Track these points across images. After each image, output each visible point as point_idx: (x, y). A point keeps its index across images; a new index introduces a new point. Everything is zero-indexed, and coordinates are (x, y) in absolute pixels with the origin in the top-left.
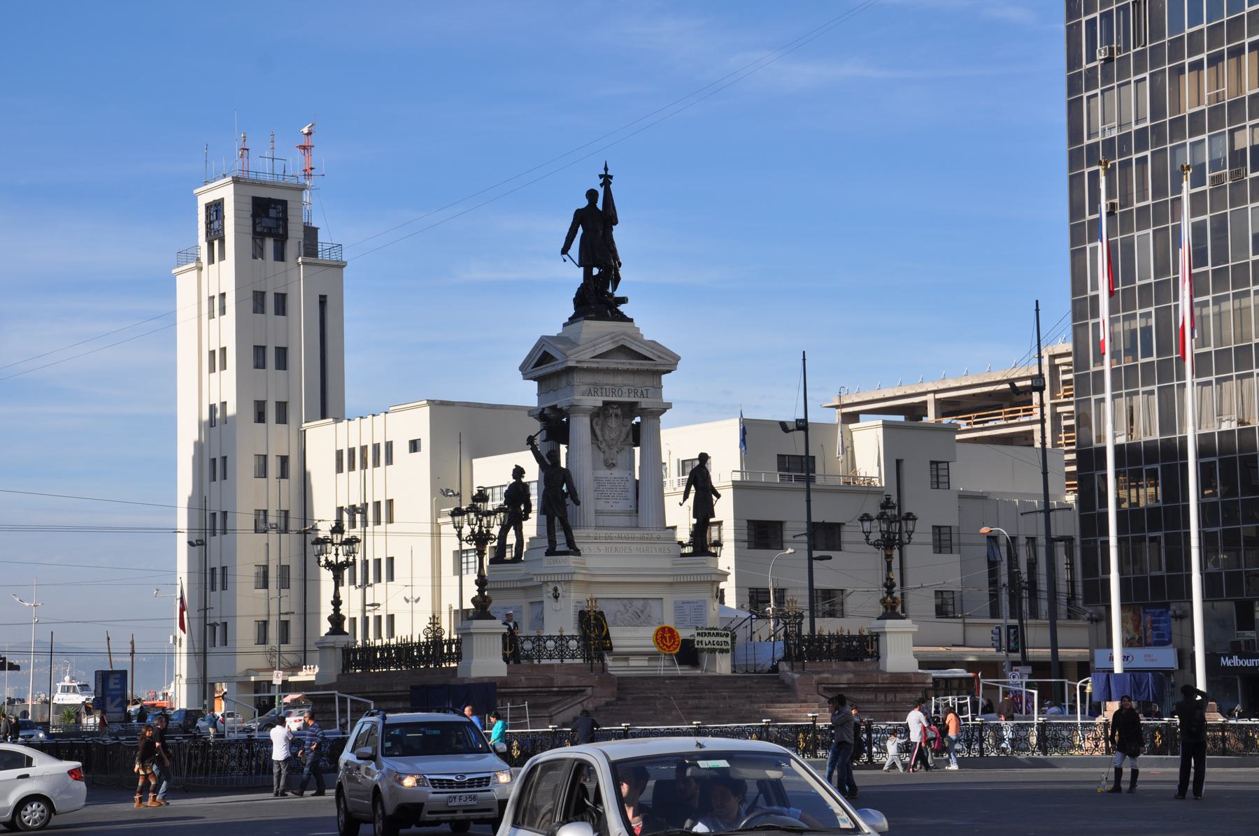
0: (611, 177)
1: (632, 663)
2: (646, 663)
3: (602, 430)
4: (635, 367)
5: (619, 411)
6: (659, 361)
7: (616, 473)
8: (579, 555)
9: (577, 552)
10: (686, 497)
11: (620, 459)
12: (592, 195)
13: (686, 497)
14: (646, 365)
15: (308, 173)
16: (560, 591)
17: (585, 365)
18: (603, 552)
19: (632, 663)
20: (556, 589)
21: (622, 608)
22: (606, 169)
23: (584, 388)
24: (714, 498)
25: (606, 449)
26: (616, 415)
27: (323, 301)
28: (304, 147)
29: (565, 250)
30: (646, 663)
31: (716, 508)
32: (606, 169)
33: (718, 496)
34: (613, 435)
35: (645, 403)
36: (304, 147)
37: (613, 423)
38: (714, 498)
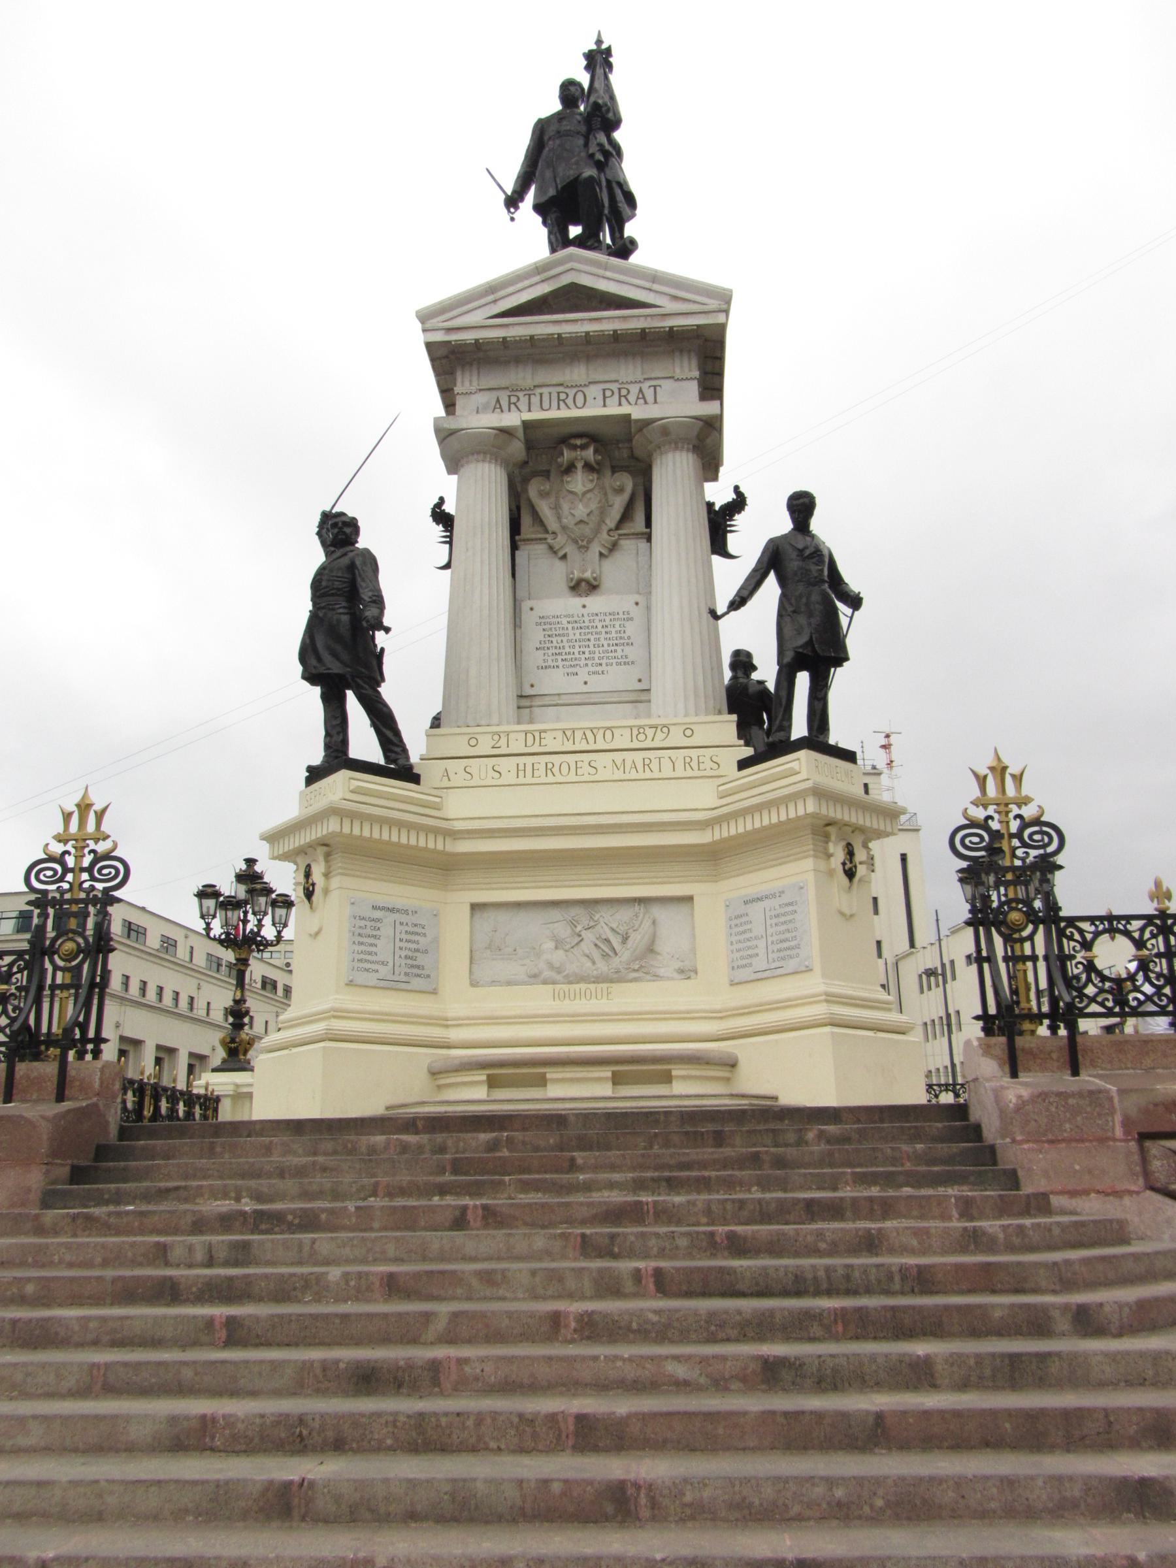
0: (608, 52)
1: (554, 1091)
2: (606, 1090)
3: (556, 508)
4: (608, 327)
5: (589, 454)
6: (670, 306)
7: (595, 603)
8: (415, 779)
9: (408, 774)
10: (738, 603)
11: (616, 571)
12: (569, 92)
13: (738, 603)
14: (633, 321)
15: (890, 764)
16: (317, 876)
17: (469, 336)
18: (511, 778)
19: (553, 1091)
20: (308, 875)
21: (564, 931)
22: (599, 42)
23: (481, 399)
24: (843, 609)
25: (569, 549)
26: (588, 467)
27: (904, 858)
28: (884, 747)
29: (512, 202)
30: (606, 1090)
31: (852, 643)
32: (599, 42)
33: (855, 602)
34: (581, 510)
35: (638, 413)
36: (884, 747)
37: (579, 482)
38: (843, 609)
